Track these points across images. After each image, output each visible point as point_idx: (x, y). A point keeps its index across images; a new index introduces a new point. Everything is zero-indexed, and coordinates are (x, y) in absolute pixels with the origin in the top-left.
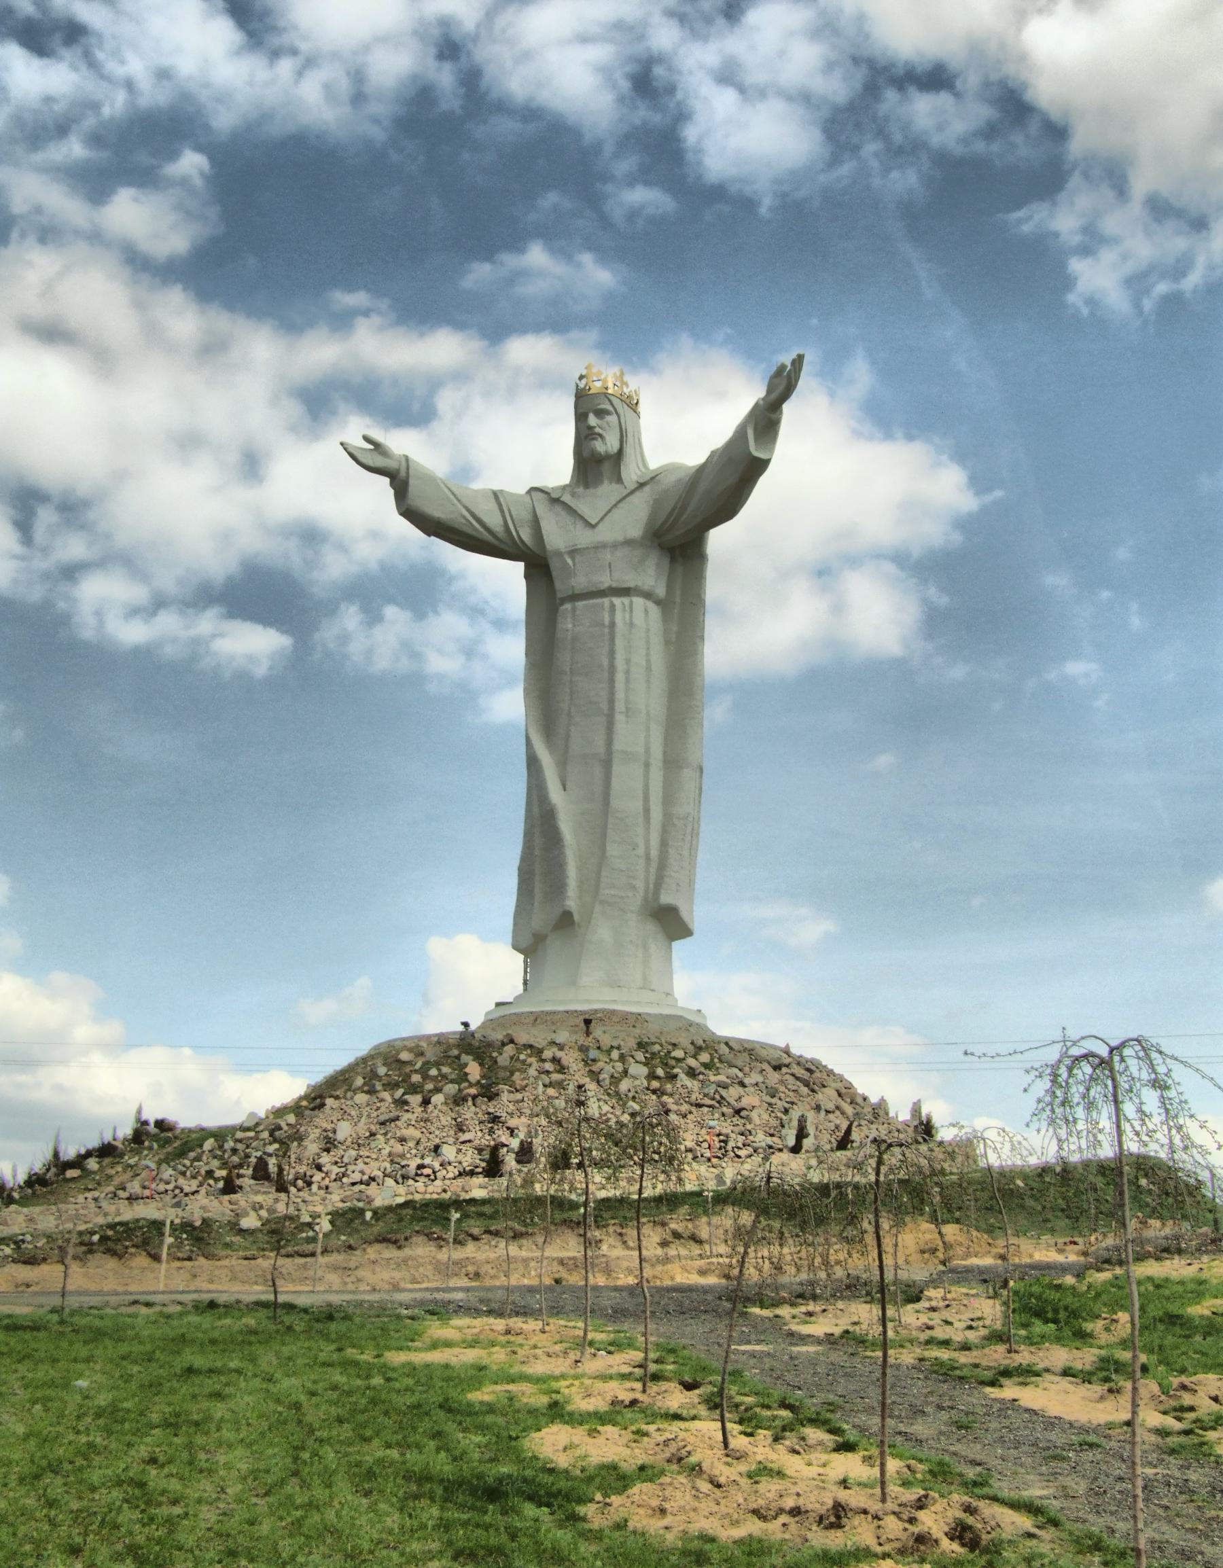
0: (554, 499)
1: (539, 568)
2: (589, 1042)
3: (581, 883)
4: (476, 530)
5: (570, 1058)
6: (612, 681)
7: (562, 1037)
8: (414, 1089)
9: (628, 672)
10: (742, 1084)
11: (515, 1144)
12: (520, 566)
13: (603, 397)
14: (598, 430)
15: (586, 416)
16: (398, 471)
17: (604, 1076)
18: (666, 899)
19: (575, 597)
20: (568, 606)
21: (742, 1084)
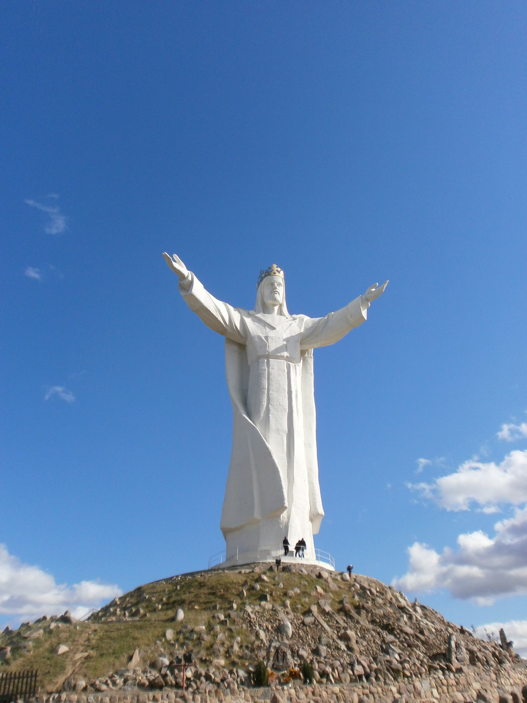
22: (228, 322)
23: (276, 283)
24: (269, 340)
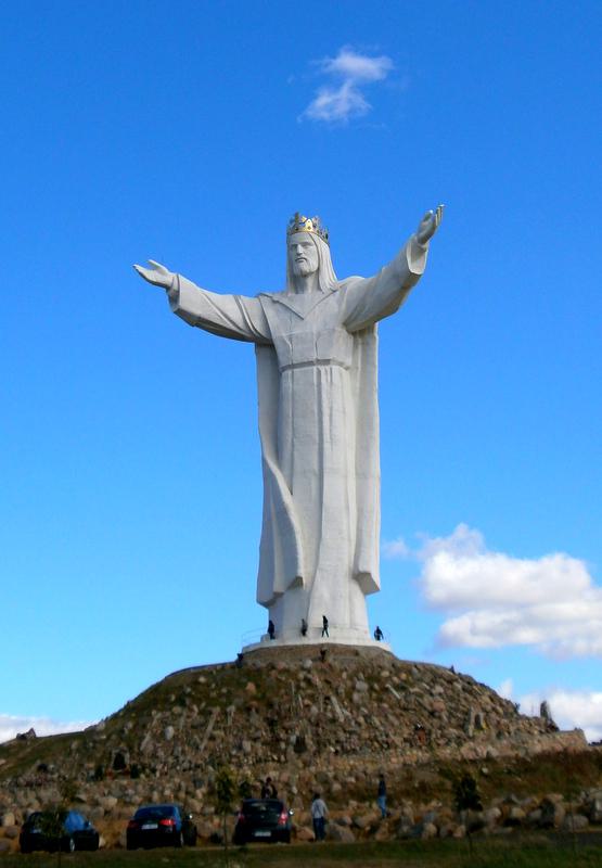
2: (324, 666)
3: (305, 559)
5: (317, 681)
6: (321, 422)
7: (309, 663)
8: (212, 702)
9: (331, 415)
10: (431, 694)
11: (293, 739)
12: (253, 344)
14: (303, 256)
15: (296, 246)
17: (341, 690)
18: (362, 568)
19: (293, 366)
20: (290, 372)
21: (431, 694)
22: (241, 325)
23: (299, 246)
24: (294, 341)
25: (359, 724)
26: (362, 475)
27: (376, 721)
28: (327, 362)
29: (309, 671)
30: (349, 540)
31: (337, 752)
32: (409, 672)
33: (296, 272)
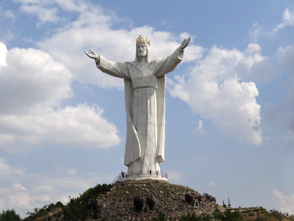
0: (131, 64)
1: (128, 80)
4: (115, 72)
13: (143, 43)
14: (142, 50)
15: (139, 47)
16: (97, 58)
18: (159, 155)
20: (136, 90)
21: (182, 195)
22: (120, 73)
25: (162, 204)
26: (160, 125)
27: (167, 203)
28: (149, 87)
29: (145, 187)
30: (155, 146)
31: (156, 212)
32: (175, 188)
33: (139, 55)
